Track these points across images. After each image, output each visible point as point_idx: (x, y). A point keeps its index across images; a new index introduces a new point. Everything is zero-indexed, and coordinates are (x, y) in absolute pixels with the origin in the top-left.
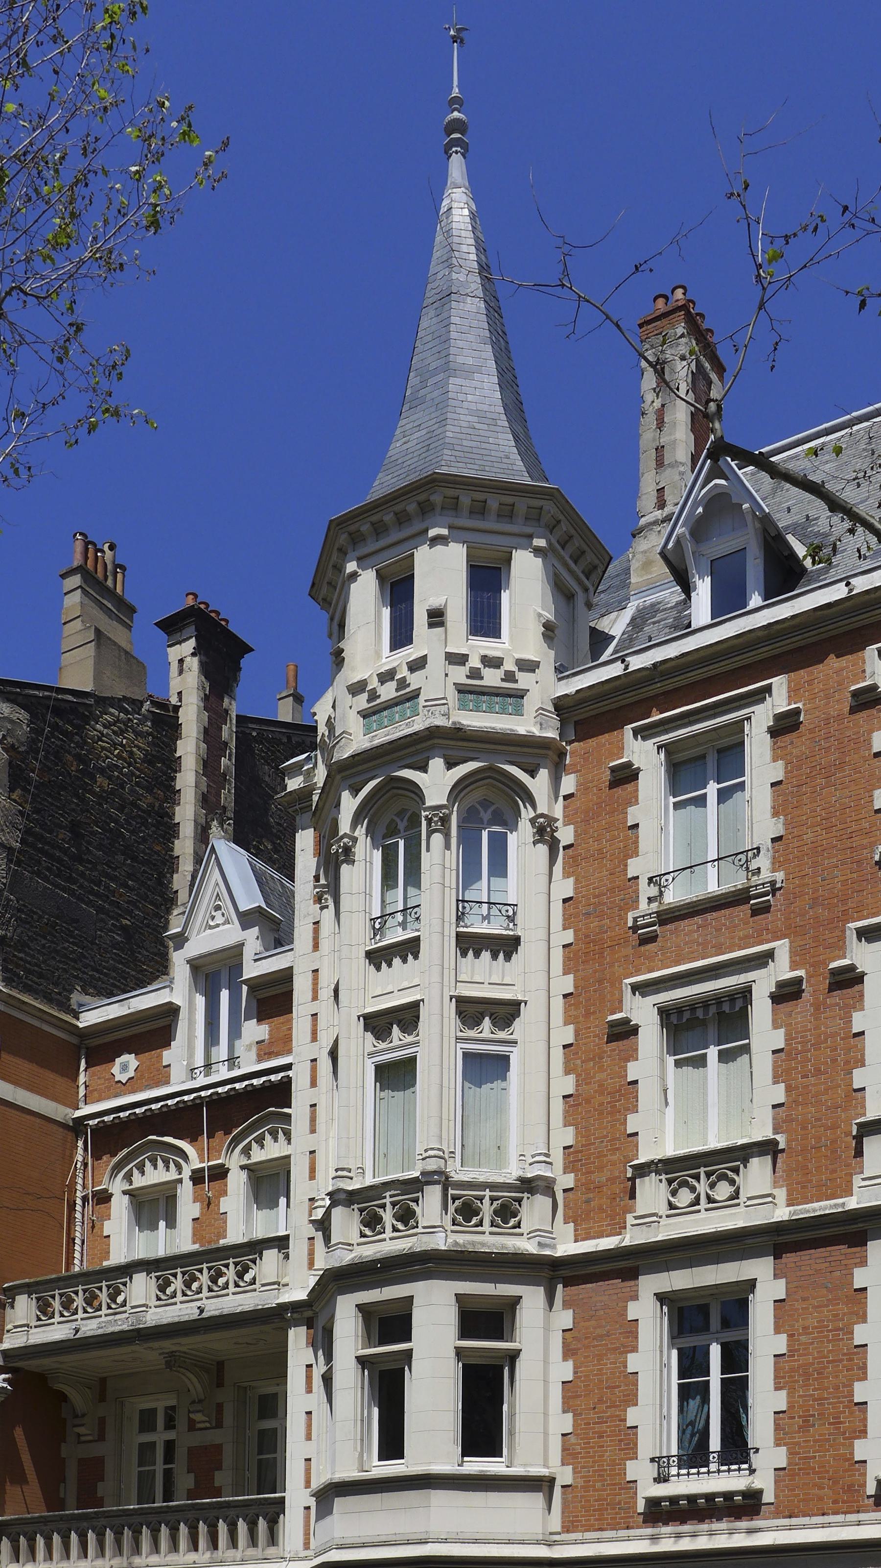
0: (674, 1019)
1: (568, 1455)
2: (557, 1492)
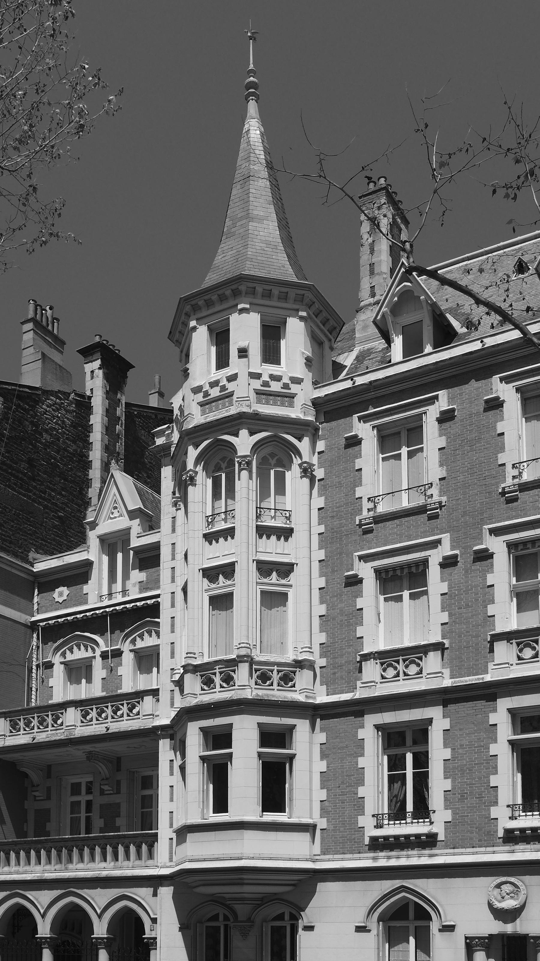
0: (383, 575)
1: (324, 812)
2: (318, 832)
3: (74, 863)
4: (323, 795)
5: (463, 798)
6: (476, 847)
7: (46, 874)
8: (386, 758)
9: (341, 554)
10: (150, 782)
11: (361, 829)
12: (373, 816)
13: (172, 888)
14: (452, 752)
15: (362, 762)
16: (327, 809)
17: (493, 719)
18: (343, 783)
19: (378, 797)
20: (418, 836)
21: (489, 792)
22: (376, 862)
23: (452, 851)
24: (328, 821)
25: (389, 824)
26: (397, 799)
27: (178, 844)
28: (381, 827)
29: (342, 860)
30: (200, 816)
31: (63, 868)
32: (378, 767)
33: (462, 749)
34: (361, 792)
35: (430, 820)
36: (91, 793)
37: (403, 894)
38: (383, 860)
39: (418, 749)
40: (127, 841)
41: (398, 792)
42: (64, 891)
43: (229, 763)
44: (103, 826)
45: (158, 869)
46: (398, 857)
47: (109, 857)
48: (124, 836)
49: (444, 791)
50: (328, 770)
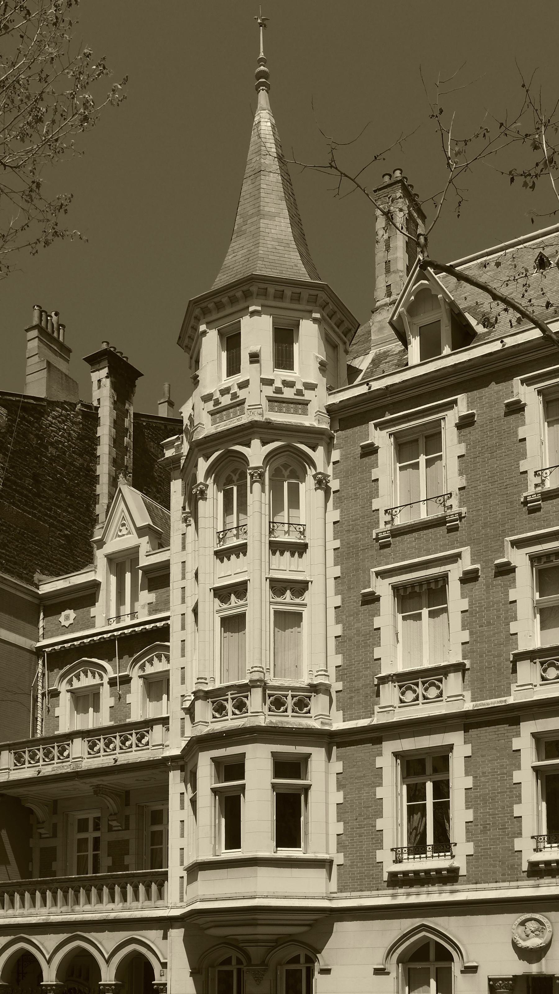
0: (402, 592)
1: (341, 846)
2: (335, 868)
3: (81, 905)
4: (340, 828)
5: (485, 830)
6: (499, 882)
7: (52, 917)
8: (405, 787)
9: (357, 570)
10: (160, 817)
11: (380, 864)
12: (392, 850)
13: (183, 930)
14: (473, 780)
15: (380, 792)
16: (344, 843)
17: (516, 744)
18: (360, 815)
19: (397, 829)
20: (438, 871)
21: (512, 823)
22: (395, 899)
23: (474, 886)
24: (345, 856)
25: (408, 859)
26: (417, 830)
27: (189, 882)
28: (401, 862)
29: (360, 897)
30: (212, 852)
31: (70, 911)
32: (397, 798)
33: (484, 776)
34: (380, 824)
35: (452, 854)
36: (99, 829)
37: (424, 933)
38: (404, 897)
39: (439, 777)
40: (135, 880)
41: (418, 824)
42: (70, 935)
43: (242, 795)
44: (111, 864)
45: (168, 910)
46: (418, 894)
47: (117, 898)
48: (133, 875)
49: (466, 822)
50: (344, 801)
